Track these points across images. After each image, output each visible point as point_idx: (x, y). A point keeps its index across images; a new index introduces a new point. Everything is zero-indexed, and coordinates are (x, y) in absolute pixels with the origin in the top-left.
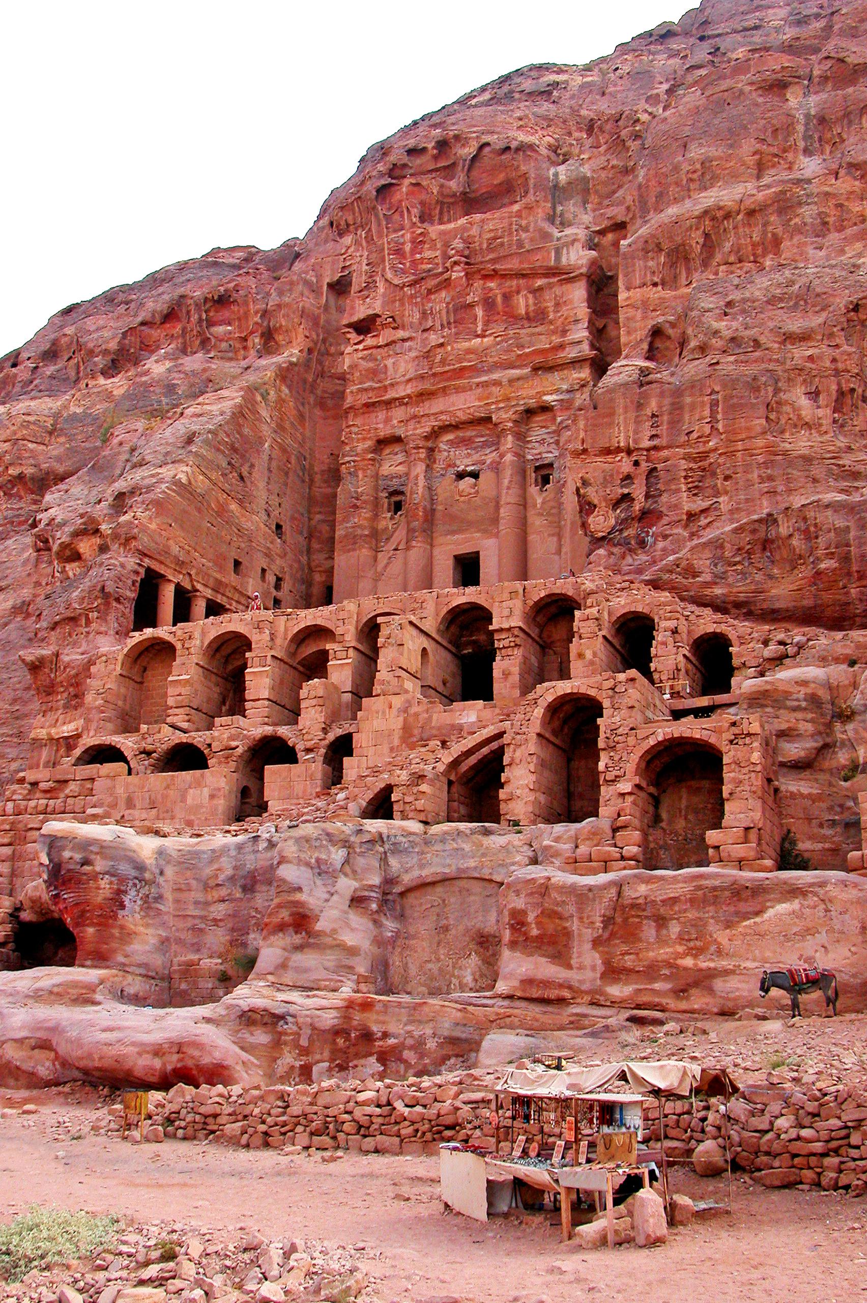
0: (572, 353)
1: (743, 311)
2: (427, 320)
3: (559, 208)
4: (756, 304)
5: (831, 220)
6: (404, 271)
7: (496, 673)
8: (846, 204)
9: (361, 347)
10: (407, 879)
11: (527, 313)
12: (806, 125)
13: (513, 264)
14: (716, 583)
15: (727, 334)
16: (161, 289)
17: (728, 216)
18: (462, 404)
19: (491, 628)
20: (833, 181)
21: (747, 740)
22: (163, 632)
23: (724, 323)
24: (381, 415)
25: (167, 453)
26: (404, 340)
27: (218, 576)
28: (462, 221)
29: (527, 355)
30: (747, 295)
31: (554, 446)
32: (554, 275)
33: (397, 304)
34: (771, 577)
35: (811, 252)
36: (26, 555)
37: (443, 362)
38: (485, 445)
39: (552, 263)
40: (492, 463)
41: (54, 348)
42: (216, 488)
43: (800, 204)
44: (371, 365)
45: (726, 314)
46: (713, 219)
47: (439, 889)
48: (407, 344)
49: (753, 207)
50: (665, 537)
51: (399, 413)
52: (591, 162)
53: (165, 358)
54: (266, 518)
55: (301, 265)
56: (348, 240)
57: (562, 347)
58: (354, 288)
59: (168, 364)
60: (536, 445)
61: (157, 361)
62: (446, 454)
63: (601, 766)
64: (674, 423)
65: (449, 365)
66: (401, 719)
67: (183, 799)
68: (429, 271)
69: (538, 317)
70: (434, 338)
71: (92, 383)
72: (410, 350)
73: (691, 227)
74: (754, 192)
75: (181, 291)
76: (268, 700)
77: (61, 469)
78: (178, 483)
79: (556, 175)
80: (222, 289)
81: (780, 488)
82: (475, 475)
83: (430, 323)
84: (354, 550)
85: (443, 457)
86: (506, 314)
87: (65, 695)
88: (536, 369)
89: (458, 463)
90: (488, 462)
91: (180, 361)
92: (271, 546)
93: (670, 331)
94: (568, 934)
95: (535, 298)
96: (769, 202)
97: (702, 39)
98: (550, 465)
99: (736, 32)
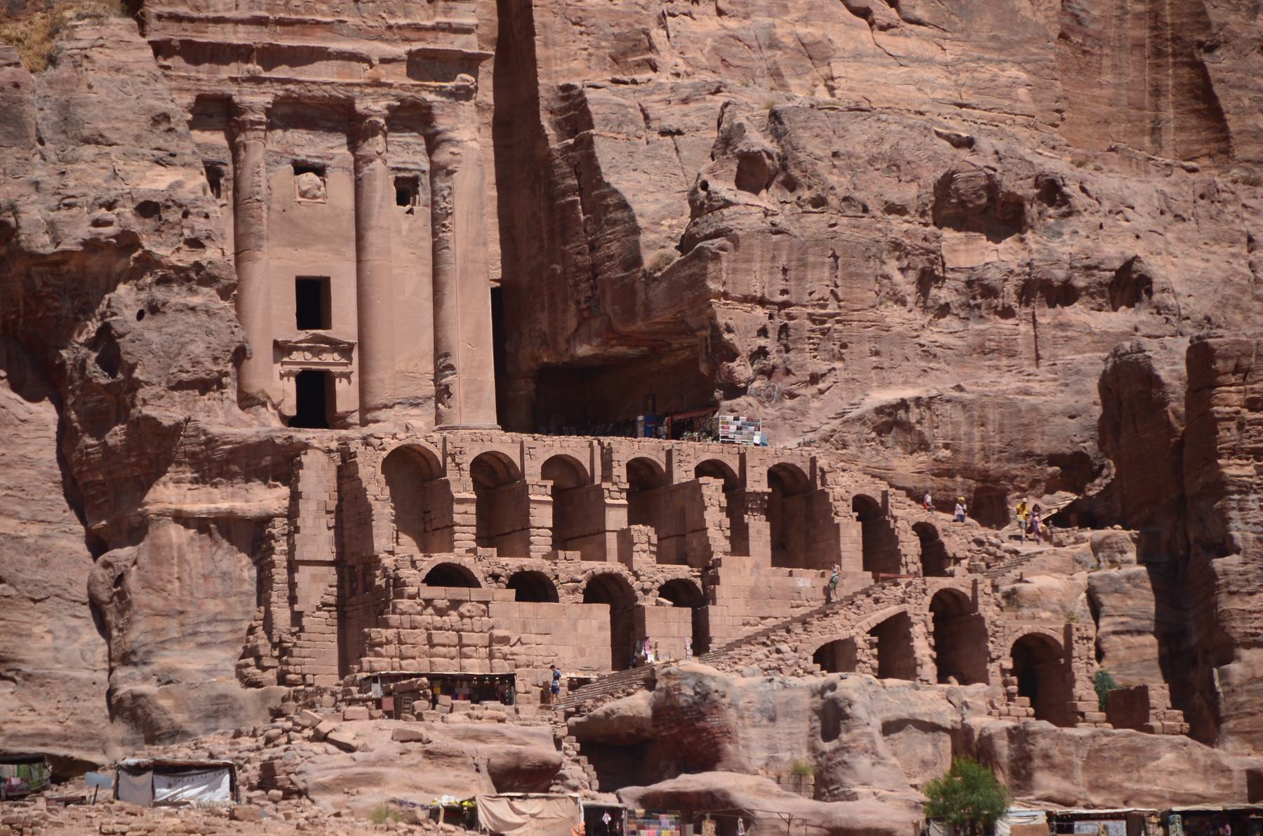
1: (850, 168)
4: (860, 161)
15: (841, 192)
29: (400, 27)
50: (792, 396)
60: (399, 149)
64: (800, 279)
66: (753, 579)
67: (575, 629)
81: (886, 365)
82: (320, 171)
93: (768, 161)
98: (414, 181)
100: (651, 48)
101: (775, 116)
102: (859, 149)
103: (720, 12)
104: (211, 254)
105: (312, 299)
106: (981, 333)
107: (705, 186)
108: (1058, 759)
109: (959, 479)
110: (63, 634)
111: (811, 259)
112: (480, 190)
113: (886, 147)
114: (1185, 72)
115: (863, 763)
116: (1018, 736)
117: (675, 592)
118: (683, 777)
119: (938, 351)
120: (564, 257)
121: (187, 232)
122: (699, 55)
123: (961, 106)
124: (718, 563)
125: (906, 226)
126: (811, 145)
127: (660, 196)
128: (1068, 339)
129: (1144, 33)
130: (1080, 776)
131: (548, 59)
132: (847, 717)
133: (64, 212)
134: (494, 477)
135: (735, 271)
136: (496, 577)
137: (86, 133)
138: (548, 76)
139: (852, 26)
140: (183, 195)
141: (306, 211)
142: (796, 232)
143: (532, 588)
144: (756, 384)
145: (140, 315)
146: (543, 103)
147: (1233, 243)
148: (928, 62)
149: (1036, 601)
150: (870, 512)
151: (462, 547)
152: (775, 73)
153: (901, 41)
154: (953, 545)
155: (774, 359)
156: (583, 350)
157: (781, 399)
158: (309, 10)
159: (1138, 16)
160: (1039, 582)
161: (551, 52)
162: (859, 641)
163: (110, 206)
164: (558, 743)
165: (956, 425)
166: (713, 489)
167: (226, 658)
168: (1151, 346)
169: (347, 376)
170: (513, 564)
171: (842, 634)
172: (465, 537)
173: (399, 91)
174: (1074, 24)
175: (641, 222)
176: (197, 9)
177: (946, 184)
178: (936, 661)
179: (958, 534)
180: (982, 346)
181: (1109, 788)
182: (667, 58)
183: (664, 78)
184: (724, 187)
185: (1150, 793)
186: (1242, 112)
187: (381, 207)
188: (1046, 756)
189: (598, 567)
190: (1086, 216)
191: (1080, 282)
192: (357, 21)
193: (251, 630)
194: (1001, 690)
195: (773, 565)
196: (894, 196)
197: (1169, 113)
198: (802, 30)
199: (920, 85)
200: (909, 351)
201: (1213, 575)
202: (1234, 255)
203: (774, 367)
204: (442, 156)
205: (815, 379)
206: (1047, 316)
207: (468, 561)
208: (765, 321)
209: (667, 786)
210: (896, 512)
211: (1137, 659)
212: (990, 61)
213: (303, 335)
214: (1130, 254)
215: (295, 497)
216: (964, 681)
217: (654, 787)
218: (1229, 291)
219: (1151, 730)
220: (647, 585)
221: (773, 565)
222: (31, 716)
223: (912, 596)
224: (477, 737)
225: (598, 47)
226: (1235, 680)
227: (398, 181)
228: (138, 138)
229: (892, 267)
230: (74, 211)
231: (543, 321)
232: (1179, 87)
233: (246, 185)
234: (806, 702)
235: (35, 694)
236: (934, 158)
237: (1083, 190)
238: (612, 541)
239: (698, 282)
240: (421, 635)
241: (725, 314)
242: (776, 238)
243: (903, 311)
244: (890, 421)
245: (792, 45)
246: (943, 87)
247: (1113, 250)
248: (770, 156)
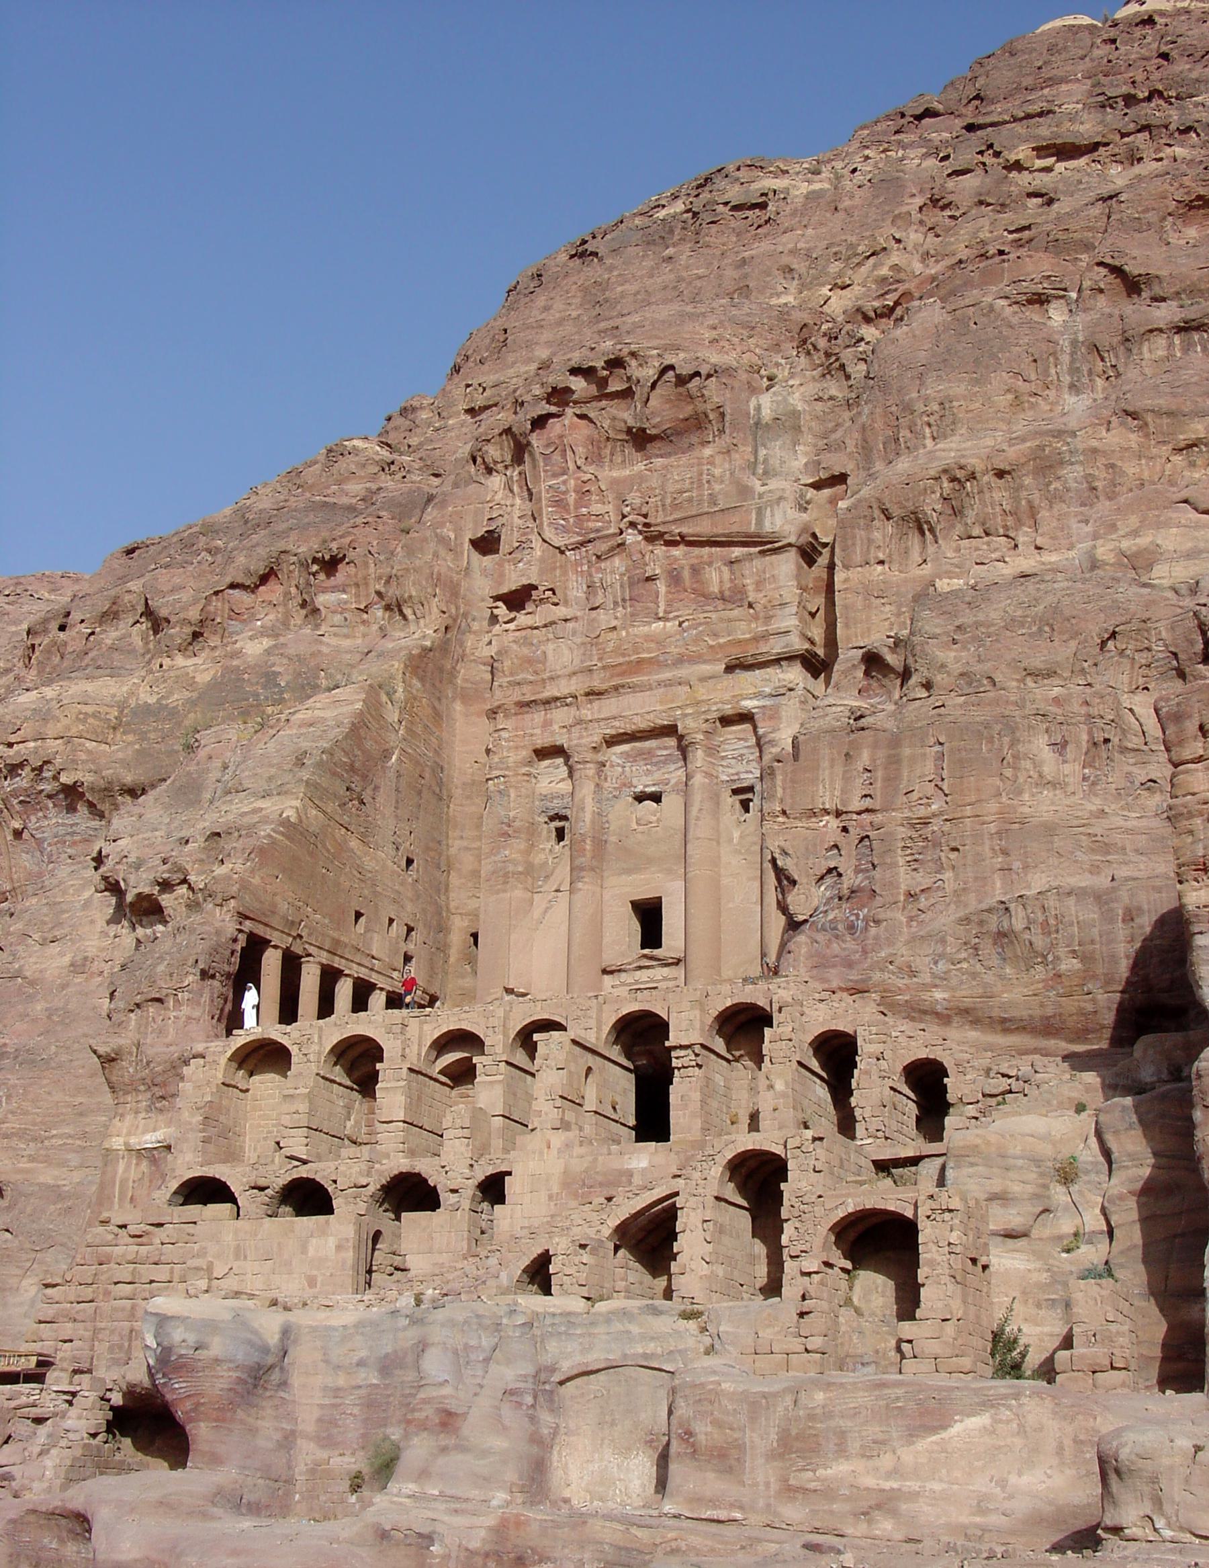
0: (776, 647)
1: (975, 638)
2: (596, 594)
3: (762, 452)
4: (992, 629)
5: (1099, 484)
6: (566, 530)
7: (673, 1099)
8: (1119, 463)
9: (511, 626)
10: (567, 1367)
11: (721, 592)
12: (1072, 354)
13: (703, 528)
14: (936, 986)
15: (957, 668)
16: (255, 538)
17: (972, 476)
18: (641, 709)
19: (667, 1044)
20: (1104, 433)
21: (947, 1216)
22: (277, 1033)
23: (953, 654)
24: (538, 716)
25: (270, 779)
27: (335, 935)
28: (641, 466)
29: (721, 646)
30: (981, 617)
31: (754, 764)
32: (755, 544)
33: (558, 572)
34: (1001, 977)
35: (1074, 525)
36: (87, 894)
37: (617, 651)
38: (668, 760)
39: (753, 528)
40: (676, 784)
41: (115, 608)
42: (332, 823)
43: (1061, 463)
44: (526, 651)
45: (954, 642)
46: (954, 479)
47: (601, 1376)
48: (570, 625)
49: (1002, 467)
51: (561, 715)
52: (802, 389)
53: (262, 635)
54: (393, 853)
55: (435, 513)
56: (496, 481)
57: (765, 637)
58: (504, 547)
59: (266, 643)
61: (251, 638)
62: (620, 769)
63: (784, 1240)
64: (892, 780)
65: (624, 655)
67: (304, 1250)
68: (598, 531)
69: (734, 597)
71: (167, 662)
72: (574, 633)
73: (925, 490)
75: (281, 545)
76: (405, 1122)
77: (128, 779)
78: (286, 823)
79: (758, 408)
80: (334, 546)
81: (1016, 865)
82: (656, 798)
83: (599, 600)
84: (505, 891)
85: (616, 774)
86: (694, 591)
87: (149, 1095)
88: (730, 669)
89: (635, 781)
90: (673, 782)
91: (282, 640)
92: (401, 889)
94: (741, 1448)
95: (732, 572)
96: (1023, 460)
97: (970, 128)
98: (750, 789)
99: (1015, 120)
139: (1198, 526)
155: (850, 879)
173: (720, 705)
187: (698, 819)
195: (666, 1138)
196: (1037, 662)
198: (1125, 544)
208: (838, 837)
221: (666, 1138)
225: (899, 615)
229: (1040, 745)
245: (1112, 561)
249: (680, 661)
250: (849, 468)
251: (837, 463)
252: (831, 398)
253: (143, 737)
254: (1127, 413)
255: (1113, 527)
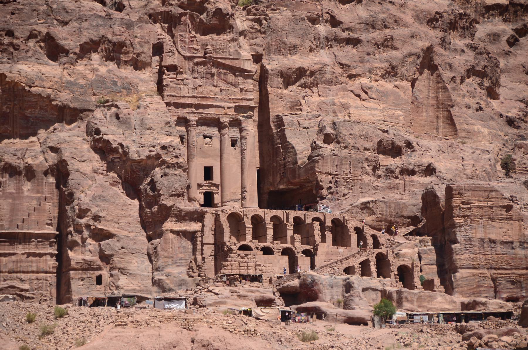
9: (169, 76)
18: (211, 112)
26: (187, 79)
29: (233, 99)
33: (183, 63)
43: (326, 73)
50: (338, 200)
64: (341, 168)
65: (203, 94)
67: (279, 262)
69: (235, 85)
70: (199, 82)
74: (313, 65)
82: (210, 138)
98: (236, 141)
100: (301, 105)
101: (334, 124)
102: (357, 133)
103: (319, 95)
104: (181, 160)
105: (208, 172)
106: (389, 183)
107: (315, 142)
108: (409, 298)
109: (383, 222)
110: (140, 262)
111: (344, 162)
112: (254, 143)
113: (364, 132)
114: (445, 113)
115: (357, 299)
116: (399, 292)
117: (306, 253)
118: (308, 303)
119: (377, 188)
120: (277, 161)
121: (174, 154)
122: (314, 107)
123: (385, 121)
124: (318, 245)
125: (369, 154)
126: (344, 132)
127: (303, 145)
128: (413, 185)
129: (434, 102)
130: (416, 304)
131: (272, 108)
132: (352, 287)
133: (141, 148)
134: (257, 221)
135: (323, 166)
136: (257, 248)
137: (147, 127)
138: (273, 112)
139: (355, 99)
140: (174, 144)
141: (207, 149)
142: (339, 155)
143: (267, 251)
144: (328, 196)
145: (162, 176)
146: (271, 120)
147: (458, 159)
148: (376, 109)
149: (404, 256)
150: (359, 232)
151: (249, 241)
152: (334, 112)
153: (368, 104)
154: (382, 240)
155: (333, 189)
156: (282, 187)
157: (335, 200)
158: (208, 94)
159: (433, 98)
160: (405, 251)
161: (273, 106)
162: (356, 266)
163: (154, 147)
164: (274, 293)
165: (383, 208)
166: (316, 225)
167: (184, 269)
168: (436, 187)
169: (218, 193)
170: (262, 245)
171: (351, 265)
172: (249, 237)
174: (415, 99)
175: (297, 152)
176: (178, 93)
177: (380, 143)
178: (377, 272)
179: (383, 238)
180: (390, 186)
181: (423, 307)
182: (305, 108)
183: (304, 113)
184: (320, 143)
185: (435, 308)
186: (461, 124)
188: (406, 298)
189: (285, 246)
190: (418, 152)
191: (417, 169)
192: (221, 97)
193: (191, 262)
194: (394, 280)
197: (441, 124)
198: (341, 100)
199: (373, 115)
200: (370, 188)
201: (452, 249)
202: (458, 163)
203: (333, 192)
204: (244, 134)
205: (344, 195)
206: (408, 178)
207: (250, 244)
208: (331, 179)
209: (303, 305)
210: (366, 231)
211: (431, 272)
212: (392, 109)
213: (206, 182)
214: (430, 162)
215: (203, 226)
216: (384, 277)
217: (300, 306)
218: (457, 172)
219: (435, 291)
220: (298, 251)
222: (131, 285)
223: (371, 255)
224: (252, 291)
225: (286, 105)
226: (458, 278)
227: (232, 141)
228: (161, 128)
229: (365, 165)
230: (144, 148)
231: (271, 179)
232: (444, 117)
233: (190, 141)
234: (341, 283)
235: (133, 279)
236: (377, 135)
237: (418, 144)
238: (289, 239)
239: (313, 168)
240: (237, 264)
241: (320, 177)
242: (334, 157)
243: (369, 177)
244: (365, 207)
246: (380, 116)
247: (426, 161)
248: (333, 134)
249: (221, 100)
250: (264, 52)
251: (260, 50)
252: (256, 29)
253: (72, 92)
254: (340, 63)
255: (337, 95)
